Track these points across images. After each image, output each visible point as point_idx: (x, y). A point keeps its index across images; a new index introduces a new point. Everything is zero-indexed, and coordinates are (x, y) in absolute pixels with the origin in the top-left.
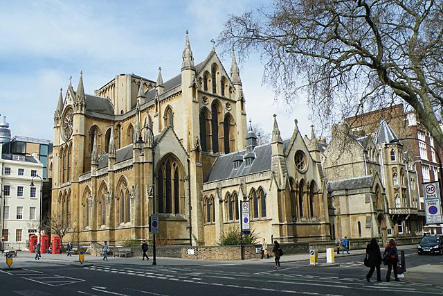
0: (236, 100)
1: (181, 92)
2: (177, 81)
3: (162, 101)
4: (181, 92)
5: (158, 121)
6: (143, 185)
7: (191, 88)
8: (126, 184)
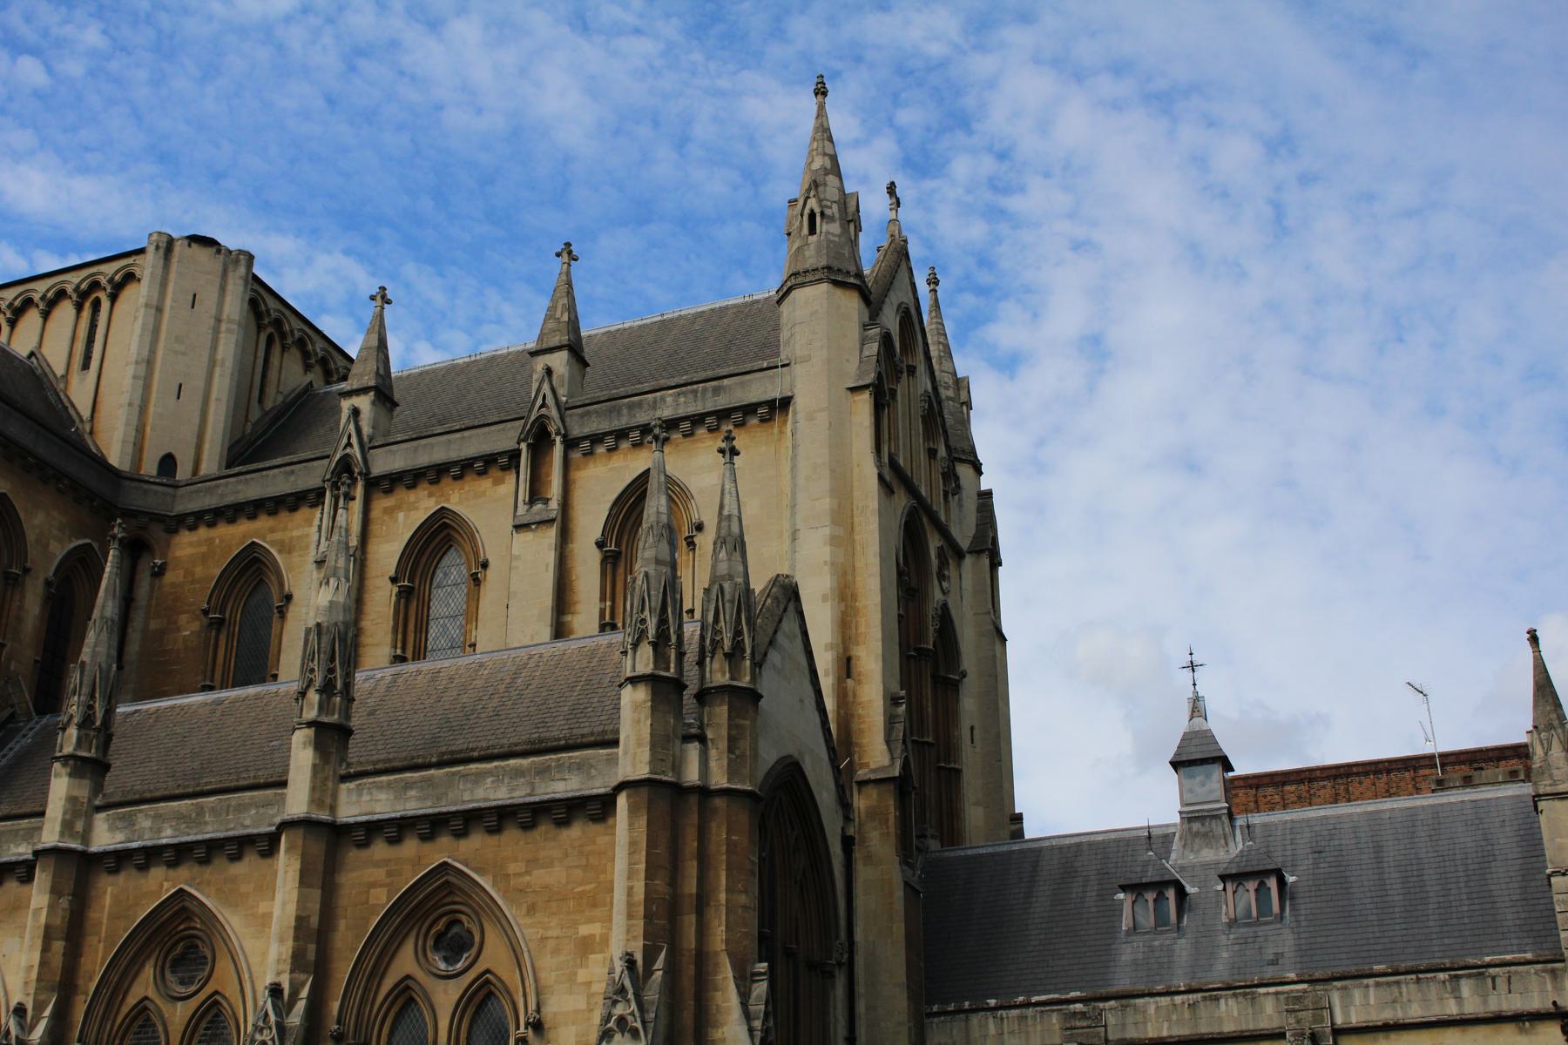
0: (965, 544)
1: (785, 403)
2: (749, 336)
3: (596, 439)
4: (785, 403)
5: (551, 557)
6: (702, 958)
7: (864, 402)
8: (455, 943)
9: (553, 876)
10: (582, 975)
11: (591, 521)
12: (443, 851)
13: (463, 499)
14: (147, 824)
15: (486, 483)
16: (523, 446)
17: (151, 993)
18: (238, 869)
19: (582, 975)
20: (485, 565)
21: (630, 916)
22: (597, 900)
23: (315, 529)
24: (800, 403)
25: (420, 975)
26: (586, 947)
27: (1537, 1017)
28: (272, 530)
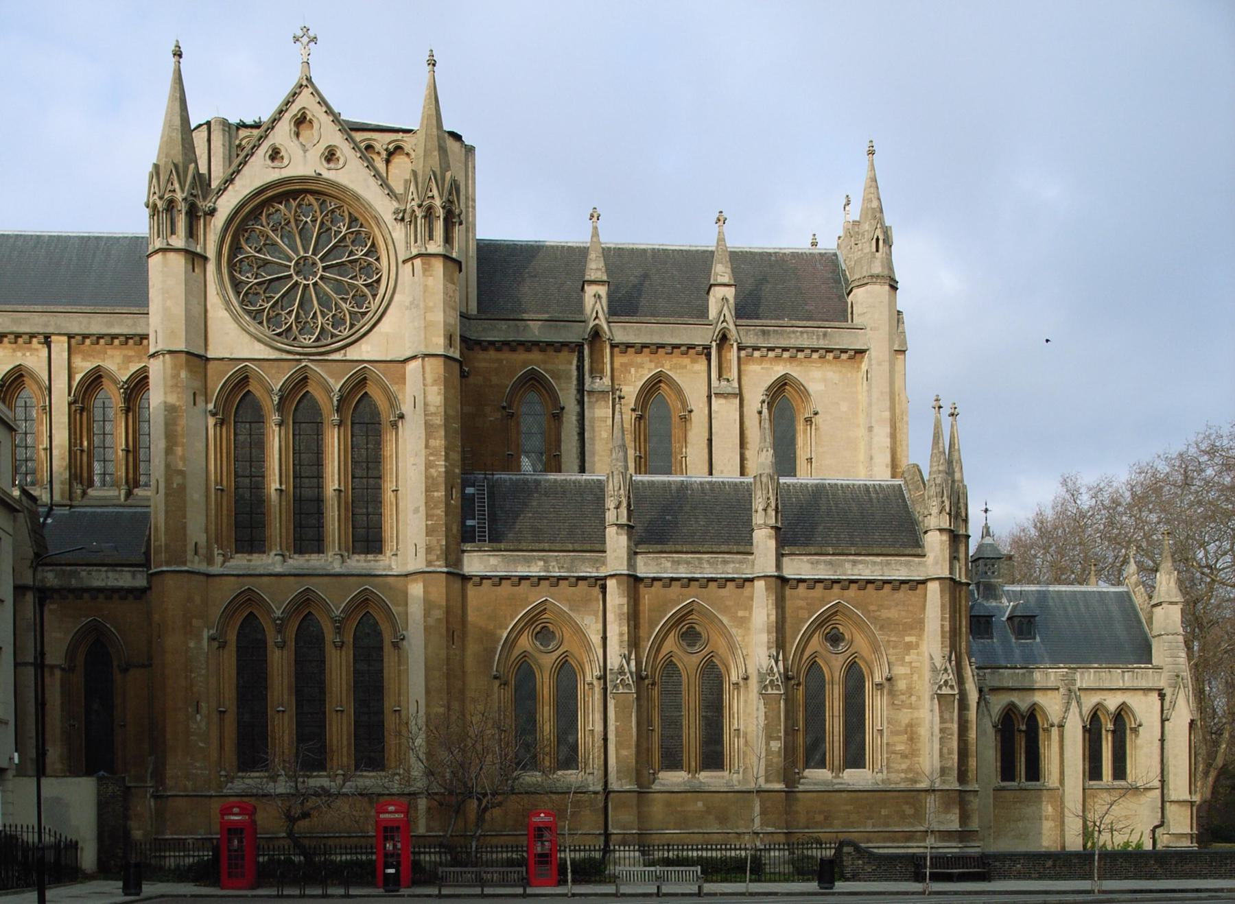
9: (892, 614)
10: (907, 659)
11: (755, 397)
12: (835, 597)
13: (669, 366)
14: (669, 564)
15: (686, 361)
16: (714, 344)
17: (675, 649)
18: (723, 592)
19: (907, 659)
20: (691, 411)
21: (943, 637)
22: (918, 625)
23: (574, 367)
24: (873, 353)
25: (824, 652)
26: (909, 647)
27: (1151, 690)
28: (545, 362)
